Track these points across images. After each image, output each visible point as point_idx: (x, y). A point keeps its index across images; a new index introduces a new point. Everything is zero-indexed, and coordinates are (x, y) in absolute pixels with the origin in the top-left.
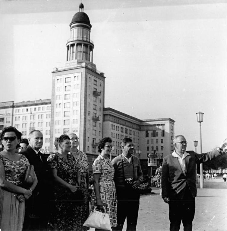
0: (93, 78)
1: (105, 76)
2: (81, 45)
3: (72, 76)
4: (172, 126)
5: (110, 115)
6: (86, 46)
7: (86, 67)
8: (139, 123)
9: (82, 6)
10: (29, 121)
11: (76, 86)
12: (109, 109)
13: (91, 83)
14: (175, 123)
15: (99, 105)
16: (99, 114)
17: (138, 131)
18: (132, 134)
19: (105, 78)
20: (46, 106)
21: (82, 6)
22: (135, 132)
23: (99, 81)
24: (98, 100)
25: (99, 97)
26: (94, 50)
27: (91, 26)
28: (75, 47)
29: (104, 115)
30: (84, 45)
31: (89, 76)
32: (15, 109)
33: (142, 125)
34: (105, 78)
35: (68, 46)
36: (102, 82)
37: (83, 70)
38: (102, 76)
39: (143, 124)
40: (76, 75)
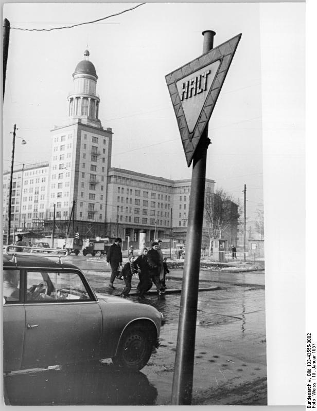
0: (90, 135)
1: (113, 132)
5: (115, 176)
8: (169, 184)
9: (88, 54)
14: (215, 184)
19: (112, 133)
21: (88, 54)
22: (162, 195)
23: (101, 138)
26: (100, 104)
27: (97, 77)
28: (80, 101)
31: (83, 133)
32: (25, 172)
34: (112, 133)
35: (72, 99)
36: (107, 139)
38: (109, 132)
39: (176, 185)
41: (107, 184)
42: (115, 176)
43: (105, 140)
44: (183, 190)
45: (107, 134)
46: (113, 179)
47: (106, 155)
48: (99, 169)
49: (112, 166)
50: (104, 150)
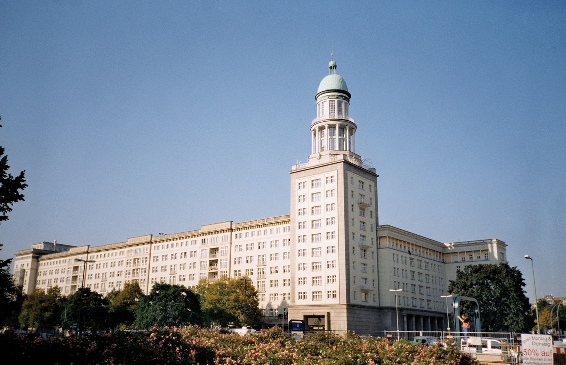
2: (335, 127)
3: (323, 177)
4: (503, 254)
6: (342, 129)
7: (346, 162)
10: (256, 252)
11: (329, 193)
12: (387, 227)
13: (355, 187)
14: (506, 247)
15: (370, 221)
16: (371, 235)
17: (440, 264)
18: (430, 270)
19: (378, 176)
20: (282, 226)
23: (368, 182)
24: (367, 213)
25: (369, 208)
29: (379, 238)
30: (339, 128)
31: (350, 174)
32: (234, 233)
33: (446, 252)
34: (378, 176)
36: (372, 184)
37: (341, 167)
38: (372, 174)
40: (329, 175)
41: (378, 248)
42: (389, 237)
43: (370, 186)
44: (467, 257)
45: (370, 177)
46: (385, 243)
47: (372, 208)
48: (368, 227)
49: (380, 224)
50: (371, 199)
